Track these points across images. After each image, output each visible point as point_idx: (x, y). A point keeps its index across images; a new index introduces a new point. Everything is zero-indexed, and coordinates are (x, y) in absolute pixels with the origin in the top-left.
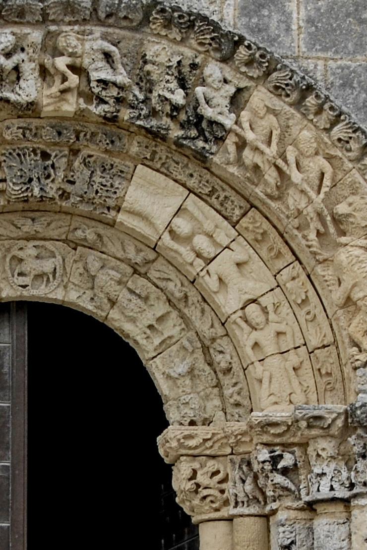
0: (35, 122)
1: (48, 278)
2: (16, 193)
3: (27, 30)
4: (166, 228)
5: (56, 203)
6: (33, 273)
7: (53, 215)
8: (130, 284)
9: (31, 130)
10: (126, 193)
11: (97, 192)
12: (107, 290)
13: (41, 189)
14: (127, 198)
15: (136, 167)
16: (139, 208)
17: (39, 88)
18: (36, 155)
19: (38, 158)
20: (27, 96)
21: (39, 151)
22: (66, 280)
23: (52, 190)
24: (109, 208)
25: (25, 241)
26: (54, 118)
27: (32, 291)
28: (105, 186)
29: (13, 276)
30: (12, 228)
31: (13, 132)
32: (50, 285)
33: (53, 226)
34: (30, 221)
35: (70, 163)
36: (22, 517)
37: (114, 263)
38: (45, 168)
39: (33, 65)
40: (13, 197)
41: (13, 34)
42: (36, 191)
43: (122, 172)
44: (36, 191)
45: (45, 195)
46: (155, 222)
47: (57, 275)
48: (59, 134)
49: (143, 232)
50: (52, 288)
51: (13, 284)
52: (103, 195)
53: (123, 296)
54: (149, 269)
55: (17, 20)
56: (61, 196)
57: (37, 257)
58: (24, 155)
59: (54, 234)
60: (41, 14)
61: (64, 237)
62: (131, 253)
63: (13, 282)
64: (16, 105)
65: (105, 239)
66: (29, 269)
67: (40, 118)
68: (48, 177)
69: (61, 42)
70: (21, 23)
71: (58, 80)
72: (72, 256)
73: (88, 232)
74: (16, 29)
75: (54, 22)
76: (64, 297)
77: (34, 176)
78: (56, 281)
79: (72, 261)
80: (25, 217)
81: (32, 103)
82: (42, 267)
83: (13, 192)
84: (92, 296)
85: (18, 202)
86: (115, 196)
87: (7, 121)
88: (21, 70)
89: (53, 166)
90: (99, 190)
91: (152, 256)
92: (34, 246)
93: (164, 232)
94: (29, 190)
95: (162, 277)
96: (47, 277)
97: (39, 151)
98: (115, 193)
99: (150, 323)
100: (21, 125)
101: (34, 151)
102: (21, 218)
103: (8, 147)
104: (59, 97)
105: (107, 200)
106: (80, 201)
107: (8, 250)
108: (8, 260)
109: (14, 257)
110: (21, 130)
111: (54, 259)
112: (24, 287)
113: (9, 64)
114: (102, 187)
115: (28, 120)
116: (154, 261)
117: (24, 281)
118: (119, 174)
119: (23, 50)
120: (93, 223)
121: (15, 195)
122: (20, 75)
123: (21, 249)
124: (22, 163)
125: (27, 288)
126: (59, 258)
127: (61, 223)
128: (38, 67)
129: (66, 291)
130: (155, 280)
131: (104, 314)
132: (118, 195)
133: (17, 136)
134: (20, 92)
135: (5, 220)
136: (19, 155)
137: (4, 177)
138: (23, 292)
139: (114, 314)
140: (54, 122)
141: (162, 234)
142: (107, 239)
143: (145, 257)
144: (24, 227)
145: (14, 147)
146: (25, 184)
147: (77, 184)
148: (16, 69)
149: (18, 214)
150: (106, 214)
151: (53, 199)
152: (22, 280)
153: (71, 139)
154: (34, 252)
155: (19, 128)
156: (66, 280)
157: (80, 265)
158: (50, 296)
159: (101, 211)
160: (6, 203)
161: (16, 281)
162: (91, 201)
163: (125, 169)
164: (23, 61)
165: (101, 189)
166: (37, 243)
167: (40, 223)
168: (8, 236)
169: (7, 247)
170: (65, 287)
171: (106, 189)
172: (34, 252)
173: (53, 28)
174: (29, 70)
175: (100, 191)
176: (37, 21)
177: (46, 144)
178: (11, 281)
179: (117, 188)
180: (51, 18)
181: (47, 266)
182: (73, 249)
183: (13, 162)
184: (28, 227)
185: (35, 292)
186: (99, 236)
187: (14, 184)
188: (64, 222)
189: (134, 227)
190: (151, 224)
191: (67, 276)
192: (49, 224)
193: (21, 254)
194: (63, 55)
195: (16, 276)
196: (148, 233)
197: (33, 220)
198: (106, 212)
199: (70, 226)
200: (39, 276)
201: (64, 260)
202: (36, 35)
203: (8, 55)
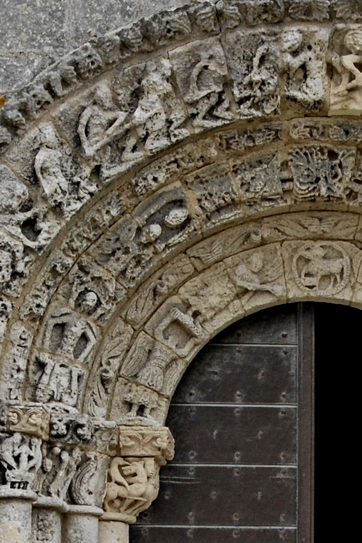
0: (322, 121)
1: (336, 279)
2: (303, 192)
3: (314, 28)
5: (343, 203)
6: (320, 273)
9: (318, 129)
13: (328, 188)
17: (326, 87)
18: (323, 154)
19: (325, 157)
20: (314, 94)
21: (326, 151)
22: (353, 280)
23: (339, 190)
25: (312, 242)
26: (342, 116)
27: (319, 291)
29: (300, 277)
31: (300, 131)
32: (337, 285)
33: (340, 225)
34: (317, 221)
35: (358, 162)
36: (309, 520)
38: (332, 168)
39: (320, 63)
40: (300, 196)
41: (300, 32)
42: (324, 191)
44: (324, 191)
45: (332, 195)
47: (345, 275)
48: (347, 132)
50: (340, 289)
51: (300, 285)
55: (304, 17)
56: (348, 196)
57: (324, 258)
58: (311, 154)
59: (342, 234)
60: (328, 12)
61: (351, 237)
63: (300, 283)
64: (303, 104)
66: (316, 269)
67: (327, 116)
68: (336, 176)
69: (349, 40)
70: (308, 21)
71: (345, 79)
74: (303, 27)
75: (341, 19)
77: (322, 175)
80: (312, 217)
81: (319, 102)
82: (330, 267)
83: (300, 192)
85: (305, 202)
87: (294, 119)
88: (308, 68)
89: (340, 165)
92: (321, 246)
94: (316, 190)
96: (334, 277)
97: (326, 151)
100: (308, 124)
101: (321, 150)
102: (308, 218)
103: (295, 146)
104: (346, 95)
107: (295, 250)
108: (295, 260)
109: (301, 258)
110: (308, 129)
111: (341, 260)
112: (311, 287)
113: (296, 62)
115: (315, 119)
117: (311, 282)
119: (310, 48)
121: (302, 194)
122: (307, 73)
123: (308, 249)
124: (309, 162)
125: (314, 289)
126: (347, 258)
127: (348, 223)
128: (325, 65)
129: (353, 292)
133: (304, 135)
134: (307, 91)
135: (291, 220)
136: (306, 154)
137: (291, 177)
138: (310, 293)
140: (341, 120)
144: (311, 227)
145: (301, 146)
146: (312, 183)
148: (303, 67)
151: (340, 198)
152: (309, 281)
153: (358, 138)
154: (321, 252)
155: (306, 127)
156: (353, 280)
158: (338, 297)
160: (293, 203)
161: (303, 281)
164: (310, 59)
166: (324, 243)
167: (327, 223)
169: (294, 247)
170: (353, 288)
172: (321, 252)
173: (340, 26)
174: (317, 68)
176: (325, 19)
177: (333, 142)
178: (298, 282)
180: (338, 16)
181: (334, 266)
183: (300, 161)
184: (315, 227)
185: (322, 293)
187: (301, 183)
188: (351, 222)
192: (336, 224)
193: (307, 254)
194: (350, 53)
195: (303, 276)
197: (320, 220)
199: (357, 226)
200: (327, 277)
201: (351, 261)
202: (323, 33)
203: (295, 53)
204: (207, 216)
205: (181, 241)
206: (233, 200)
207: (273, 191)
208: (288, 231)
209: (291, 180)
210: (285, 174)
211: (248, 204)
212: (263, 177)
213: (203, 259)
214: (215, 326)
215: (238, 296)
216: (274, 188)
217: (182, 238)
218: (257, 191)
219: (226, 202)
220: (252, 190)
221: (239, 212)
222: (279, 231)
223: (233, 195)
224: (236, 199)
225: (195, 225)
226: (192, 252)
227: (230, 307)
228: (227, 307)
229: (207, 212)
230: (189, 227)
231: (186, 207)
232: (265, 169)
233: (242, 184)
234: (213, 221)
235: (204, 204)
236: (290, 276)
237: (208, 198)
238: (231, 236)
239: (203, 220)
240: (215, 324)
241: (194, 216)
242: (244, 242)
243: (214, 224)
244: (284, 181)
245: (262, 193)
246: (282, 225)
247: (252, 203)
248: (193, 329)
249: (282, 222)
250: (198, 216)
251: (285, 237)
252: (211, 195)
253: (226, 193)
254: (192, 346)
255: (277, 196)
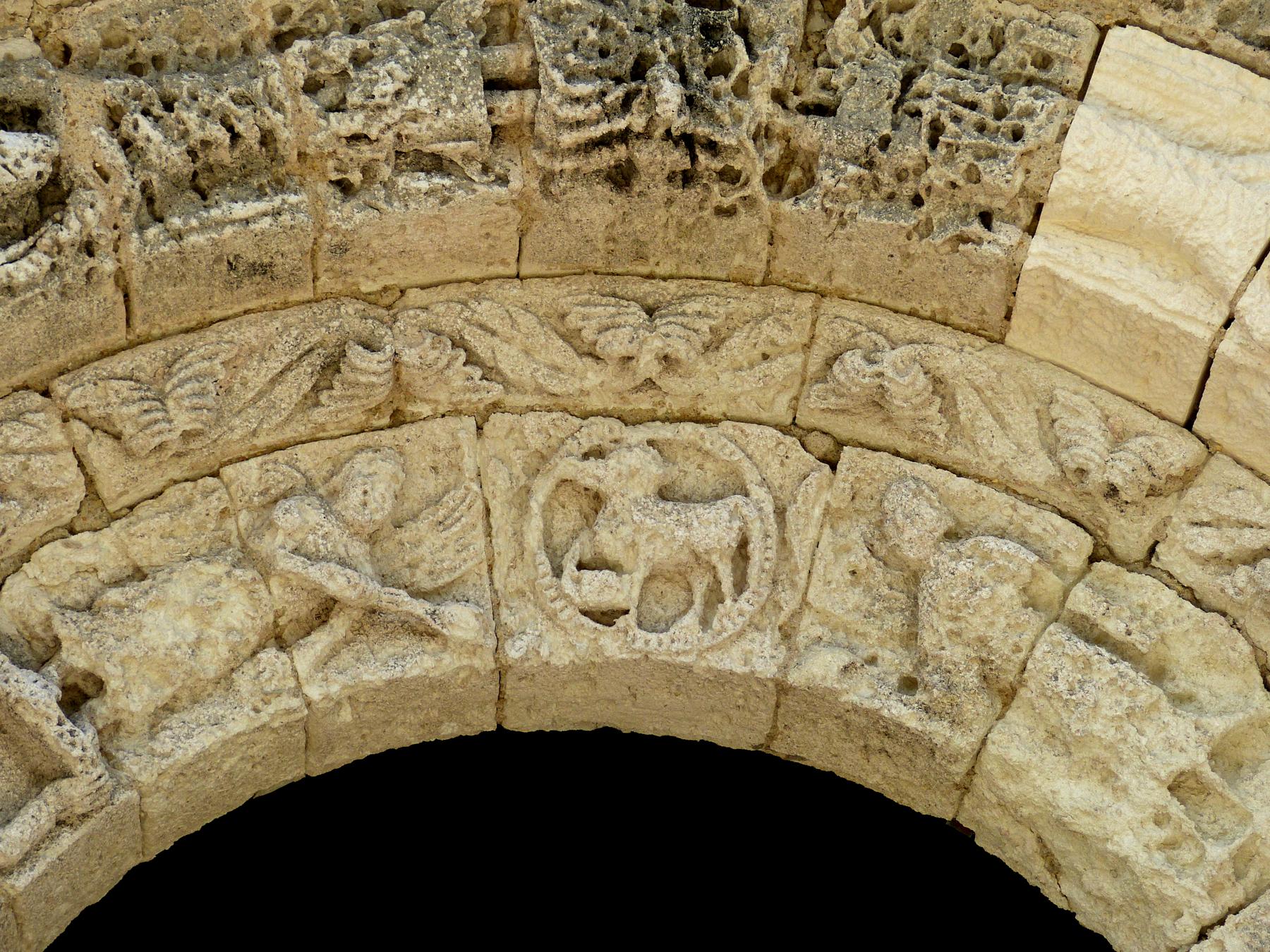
2: (579, 112)
4: (1258, 265)
7: (737, 293)
8: (1082, 600)
10: (1064, 132)
11: (936, 129)
12: (975, 625)
13: (690, 101)
14: (1070, 146)
15: (1103, 31)
16: (1130, 186)
22: (789, 600)
24: (986, 219)
25: (617, 425)
28: (973, 106)
29: (558, 572)
30: (559, 352)
34: (636, 315)
37: (999, 507)
40: (569, 139)
43: (1045, 62)
44: (670, 94)
45: (703, 130)
46: (1204, 236)
47: (753, 571)
49: (1145, 307)
51: (559, 604)
52: (966, 140)
53: (1057, 655)
54: (1166, 522)
62: (1089, 448)
65: (967, 402)
68: (719, 69)
72: (818, 493)
73: (889, 359)
76: (785, 667)
78: (746, 595)
79: (818, 512)
80: (614, 295)
84: (908, 669)
86: (1019, 147)
90: (945, 119)
91: (1179, 451)
93: (1249, 278)
95: (1227, 550)
96: (708, 579)
98: (1017, 135)
99: (1181, 762)
102: (596, 298)
105: (981, 165)
106: (860, 180)
107: (542, 460)
112: (606, 617)
114: (959, 108)
116: (1187, 478)
118: (1031, 70)
120: (914, 328)
121: (579, 124)
123: (598, 453)
125: (621, 622)
127: (770, 329)
130: (1192, 574)
131: (963, 742)
132: (1030, 141)
135: (526, 308)
139: (1013, 741)
141: (1240, 292)
142: (974, 399)
143: (1149, 456)
146: (618, 81)
147: (848, 105)
149: (587, 282)
150: (979, 242)
152: (597, 588)
156: (789, 600)
157: (855, 532)
159: (951, 232)
160: (535, 184)
162: (908, 188)
163: (1058, 45)
165: (956, 119)
166: (664, 432)
167: (680, 319)
168: (540, 390)
170: (787, 634)
171: (973, 116)
175: (951, 127)
179: (1029, 113)
181: (712, 528)
182: (823, 460)
186: (937, 381)
187: (570, 77)
188: (786, 328)
189: (1104, 288)
190: (1191, 263)
191: (793, 585)
192: (714, 344)
195: (570, 567)
196: (1175, 303)
197: (650, 312)
198: (976, 228)
199: (807, 347)
201: (780, 513)
204: (145, 187)
205: (21, 278)
206: (267, 138)
207: (450, 115)
208: (508, 359)
209: (531, 83)
210: (508, 58)
211: (335, 176)
212: (403, 51)
213: (129, 430)
214: (165, 756)
215: (280, 640)
216: (454, 99)
217: (24, 263)
218: (378, 100)
219: (235, 137)
220: (354, 98)
221: (293, 199)
222: (472, 359)
223: (269, 111)
224: (284, 134)
225: (89, 214)
226: (74, 394)
227: (243, 681)
228: (225, 680)
229: (146, 167)
230: (61, 222)
231: (48, 131)
232: (416, 27)
233: (312, 87)
234: (176, 222)
235: (136, 126)
236: (517, 580)
237: (157, 110)
238: (259, 352)
239: (127, 201)
240: (167, 749)
241: (83, 168)
242: (316, 389)
243: (179, 236)
244: (495, 85)
245: (397, 115)
246: (482, 326)
247: (356, 177)
248: (50, 730)
249: (484, 310)
250: (106, 179)
251: (496, 391)
252: (169, 107)
253: (242, 100)
254: (46, 822)
255: (465, 145)
